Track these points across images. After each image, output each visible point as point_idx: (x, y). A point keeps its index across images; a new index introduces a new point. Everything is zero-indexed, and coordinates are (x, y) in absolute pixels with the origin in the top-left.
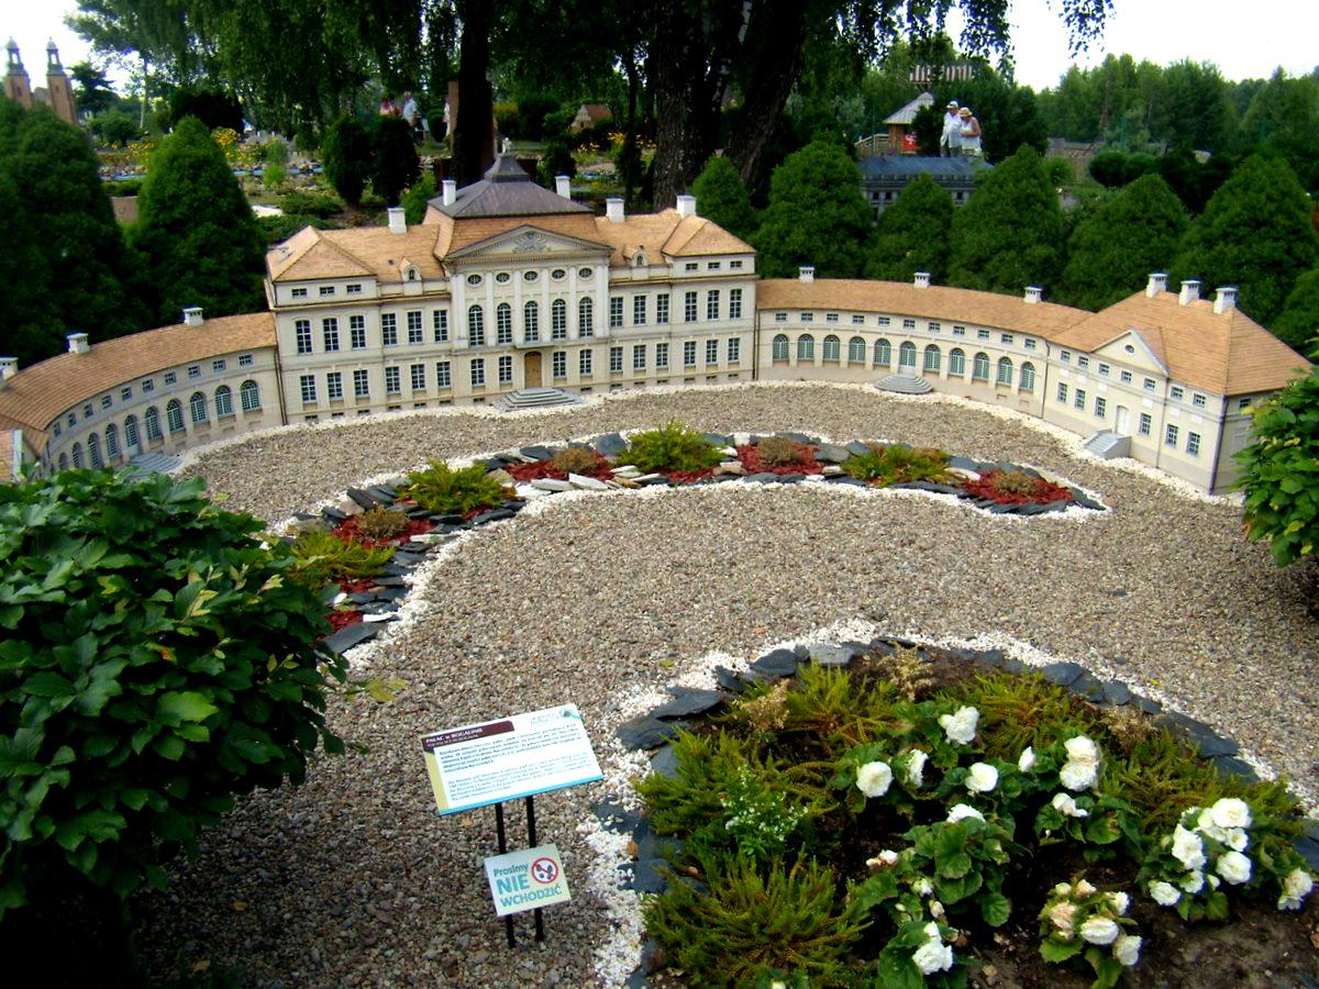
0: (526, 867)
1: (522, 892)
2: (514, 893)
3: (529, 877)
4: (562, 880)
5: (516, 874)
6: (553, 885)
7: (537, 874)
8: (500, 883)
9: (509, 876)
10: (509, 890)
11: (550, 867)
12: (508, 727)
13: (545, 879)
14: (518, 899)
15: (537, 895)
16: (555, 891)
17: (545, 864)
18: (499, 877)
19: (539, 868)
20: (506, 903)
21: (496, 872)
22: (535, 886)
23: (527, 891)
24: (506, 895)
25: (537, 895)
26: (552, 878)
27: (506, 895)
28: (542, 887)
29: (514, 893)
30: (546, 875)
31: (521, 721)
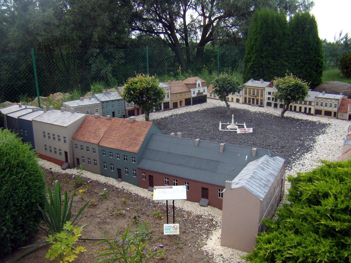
0: (171, 227)
1: (170, 231)
3: (172, 229)
4: (178, 230)
7: (173, 228)
8: (166, 229)
10: (167, 230)
15: (172, 232)
16: (176, 232)
17: (175, 227)
19: (174, 227)
21: (165, 227)
22: (172, 230)
24: (166, 231)
25: (172, 232)
27: (166, 231)
28: (174, 231)
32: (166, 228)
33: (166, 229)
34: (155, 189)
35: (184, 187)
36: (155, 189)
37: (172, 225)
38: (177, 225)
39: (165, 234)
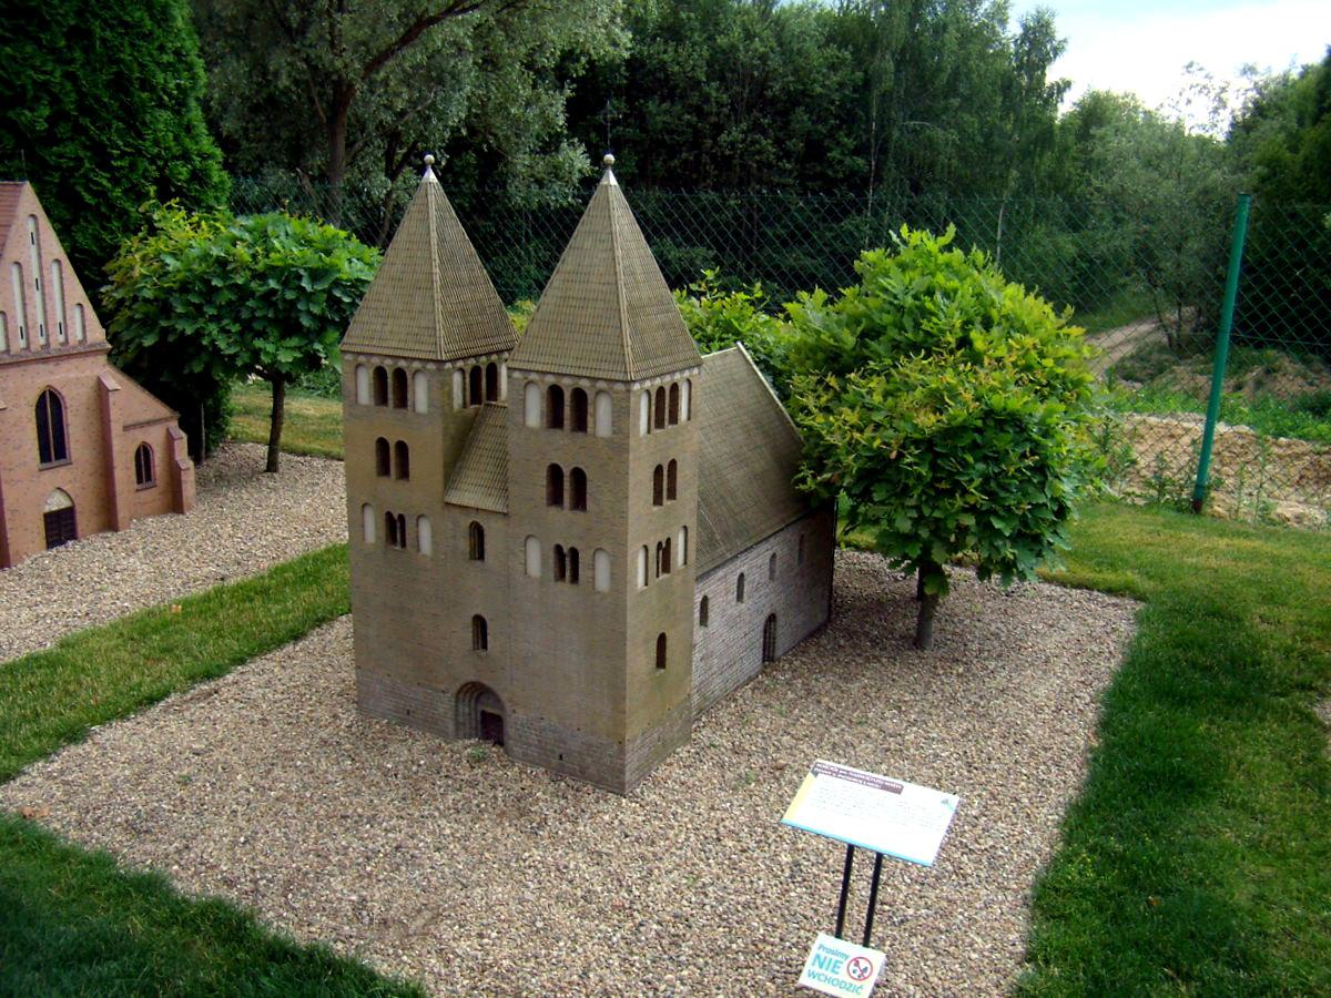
0: (847, 957)
2: (823, 971)
5: (835, 958)
6: (858, 984)
7: (852, 967)
8: (818, 956)
9: (829, 956)
11: (866, 969)
12: (898, 791)
13: (856, 975)
14: (822, 978)
15: (841, 984)
17: (863, 964)
18: (823, 954)
19: (857, 964)
20: (811, 974)
21: (821, 947)
22: (843, 975)
23: (834, 976)
24: (816, 969)
25: (841, 984)
26: (861, 978)
27: (816, 969)
28: (851, 981)
29: (823, 971)
30: (858, 972)
31: (911, 789)
32: (823, 954)
33: (818, 956)
34: (816, 774)
35: (946, 802)
36: (816, 774)
37: (856, 950)
38: (876, 958)
39: (804, 980)
